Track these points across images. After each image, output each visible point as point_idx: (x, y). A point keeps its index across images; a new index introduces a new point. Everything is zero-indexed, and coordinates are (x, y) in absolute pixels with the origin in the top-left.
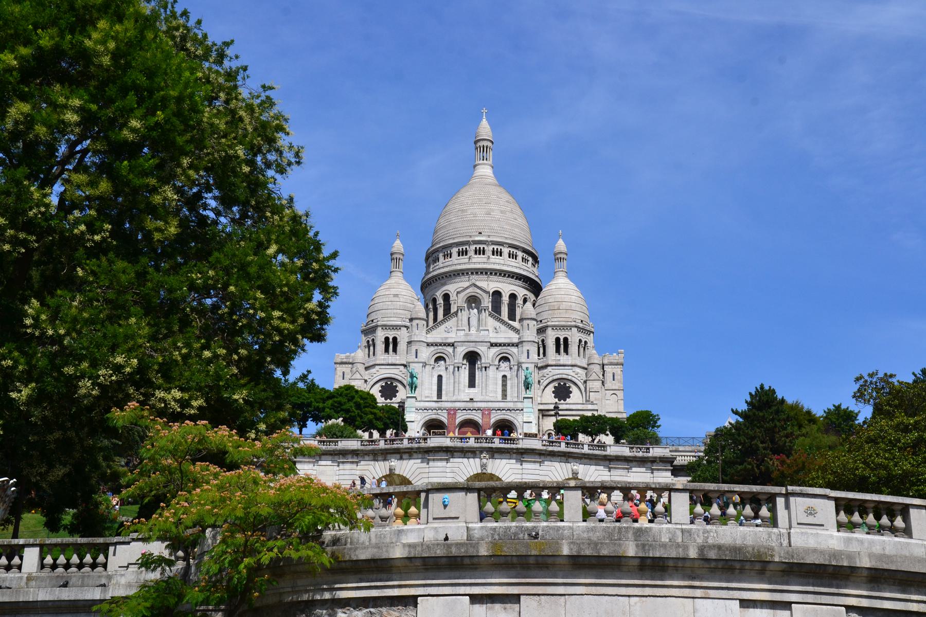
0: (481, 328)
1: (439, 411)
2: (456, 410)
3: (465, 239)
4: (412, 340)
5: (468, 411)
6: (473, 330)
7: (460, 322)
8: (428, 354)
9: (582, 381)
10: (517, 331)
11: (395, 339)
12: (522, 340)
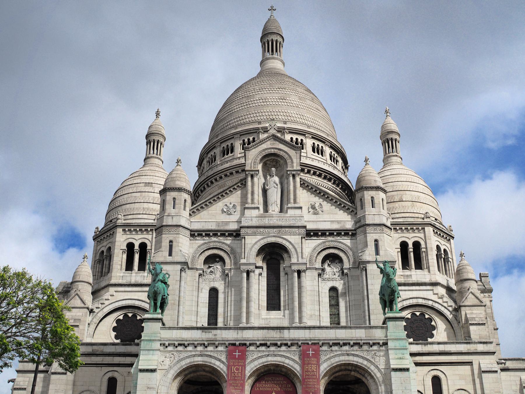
0: (289, 205)
1: (210, 348)
2: (244, 345)
3: (251, 127)
4: (164, 224)
5: (272, 348)
6: (274, 208)
7: (249, 196)
8: (192, 251)
9: (450, 309)
10: (352, 211)
11: (143, 246)
12: (362, 222)
